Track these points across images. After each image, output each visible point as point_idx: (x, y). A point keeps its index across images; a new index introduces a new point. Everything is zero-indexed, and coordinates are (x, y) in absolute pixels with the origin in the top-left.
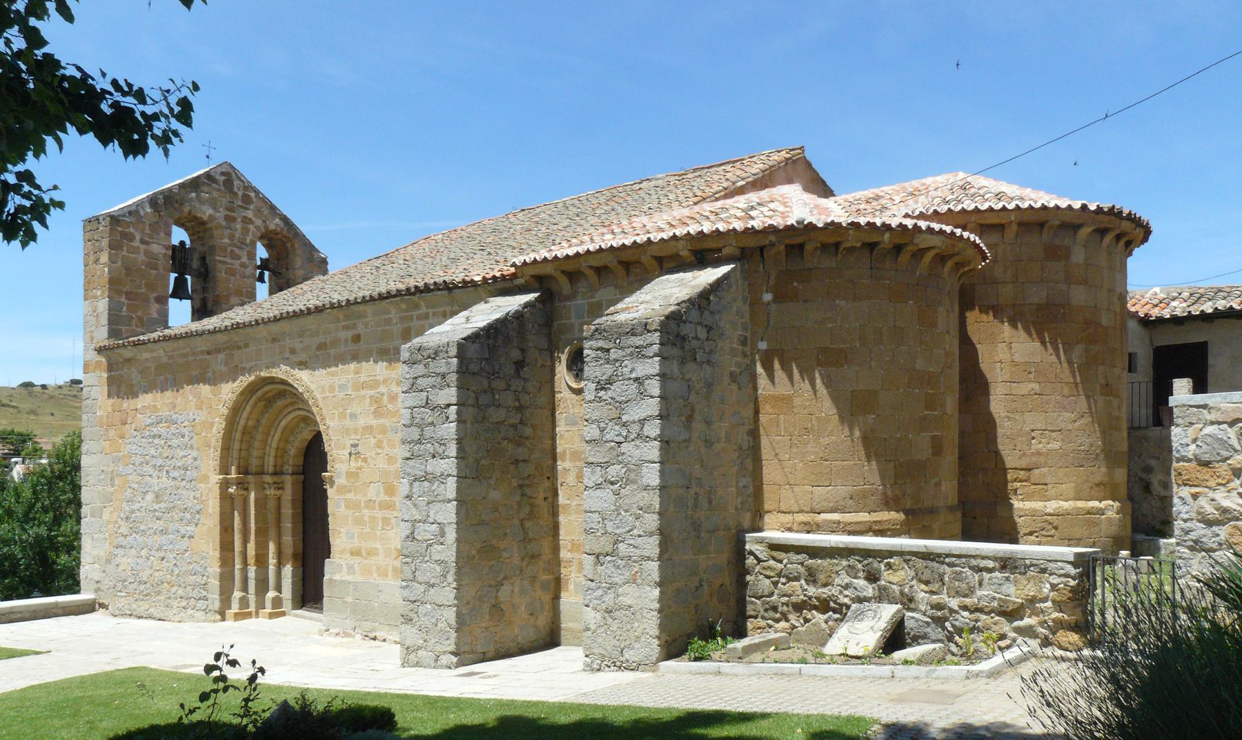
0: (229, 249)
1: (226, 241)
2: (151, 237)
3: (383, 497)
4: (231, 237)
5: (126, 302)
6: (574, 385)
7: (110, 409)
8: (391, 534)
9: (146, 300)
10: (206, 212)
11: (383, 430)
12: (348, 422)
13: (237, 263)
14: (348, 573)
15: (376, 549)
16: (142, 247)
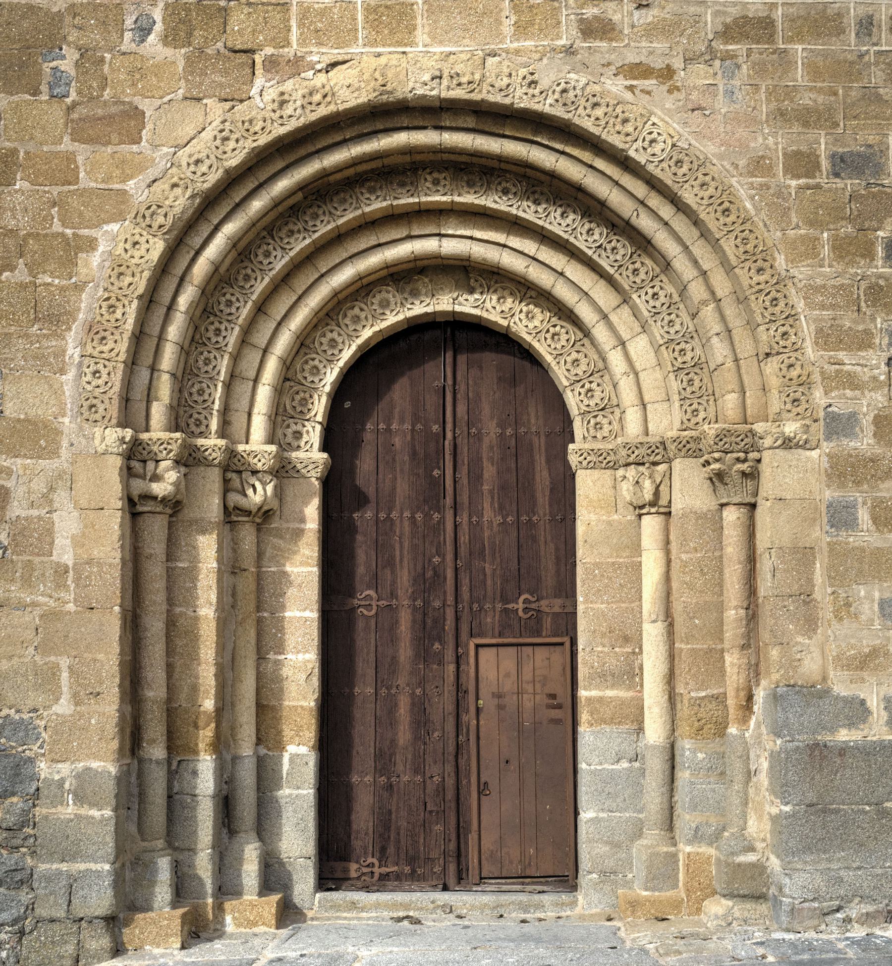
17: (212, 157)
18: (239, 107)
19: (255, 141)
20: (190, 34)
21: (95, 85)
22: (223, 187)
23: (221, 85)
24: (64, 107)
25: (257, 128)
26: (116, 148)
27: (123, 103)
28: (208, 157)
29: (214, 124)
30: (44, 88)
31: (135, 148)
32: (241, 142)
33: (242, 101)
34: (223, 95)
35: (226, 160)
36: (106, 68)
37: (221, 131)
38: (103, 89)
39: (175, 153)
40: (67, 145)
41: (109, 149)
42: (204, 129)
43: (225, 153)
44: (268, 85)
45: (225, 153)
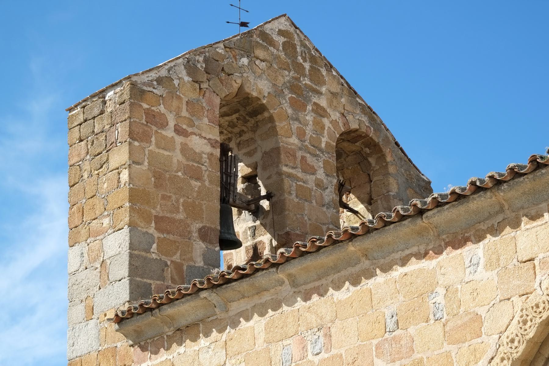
0: (299, 154)
1: (294, 140)
2: (192, 125)
4: (301, 135)
5: (156, 235)
10: (260, 87)
13: (311, 179)
16: (179, 140)
17: (519, 335)
18: (531, 297)
19: (541, 318)
20: (498, 260)
21: (455, 306)
22: (536, 350)
23: (519, 286)
24: (442, 325)
25: (541, 309)
26: (470, 343)
27: (470, 313)
28: (517, 335)
29: (518, 313)
30: (431, 316)
31: (479, 340)
32: (533, 321)
33: (531, 293)
34: (521, 293)
35: (527, 334)
36: (459, 294)
37: (522, 317)
38: (460, 308)
39: (500, 337)
40: (447, 347)
41: (467, 344)
42: (513, 317)
43: (526, 330)
44: (543, 278)
45: (526, 330)
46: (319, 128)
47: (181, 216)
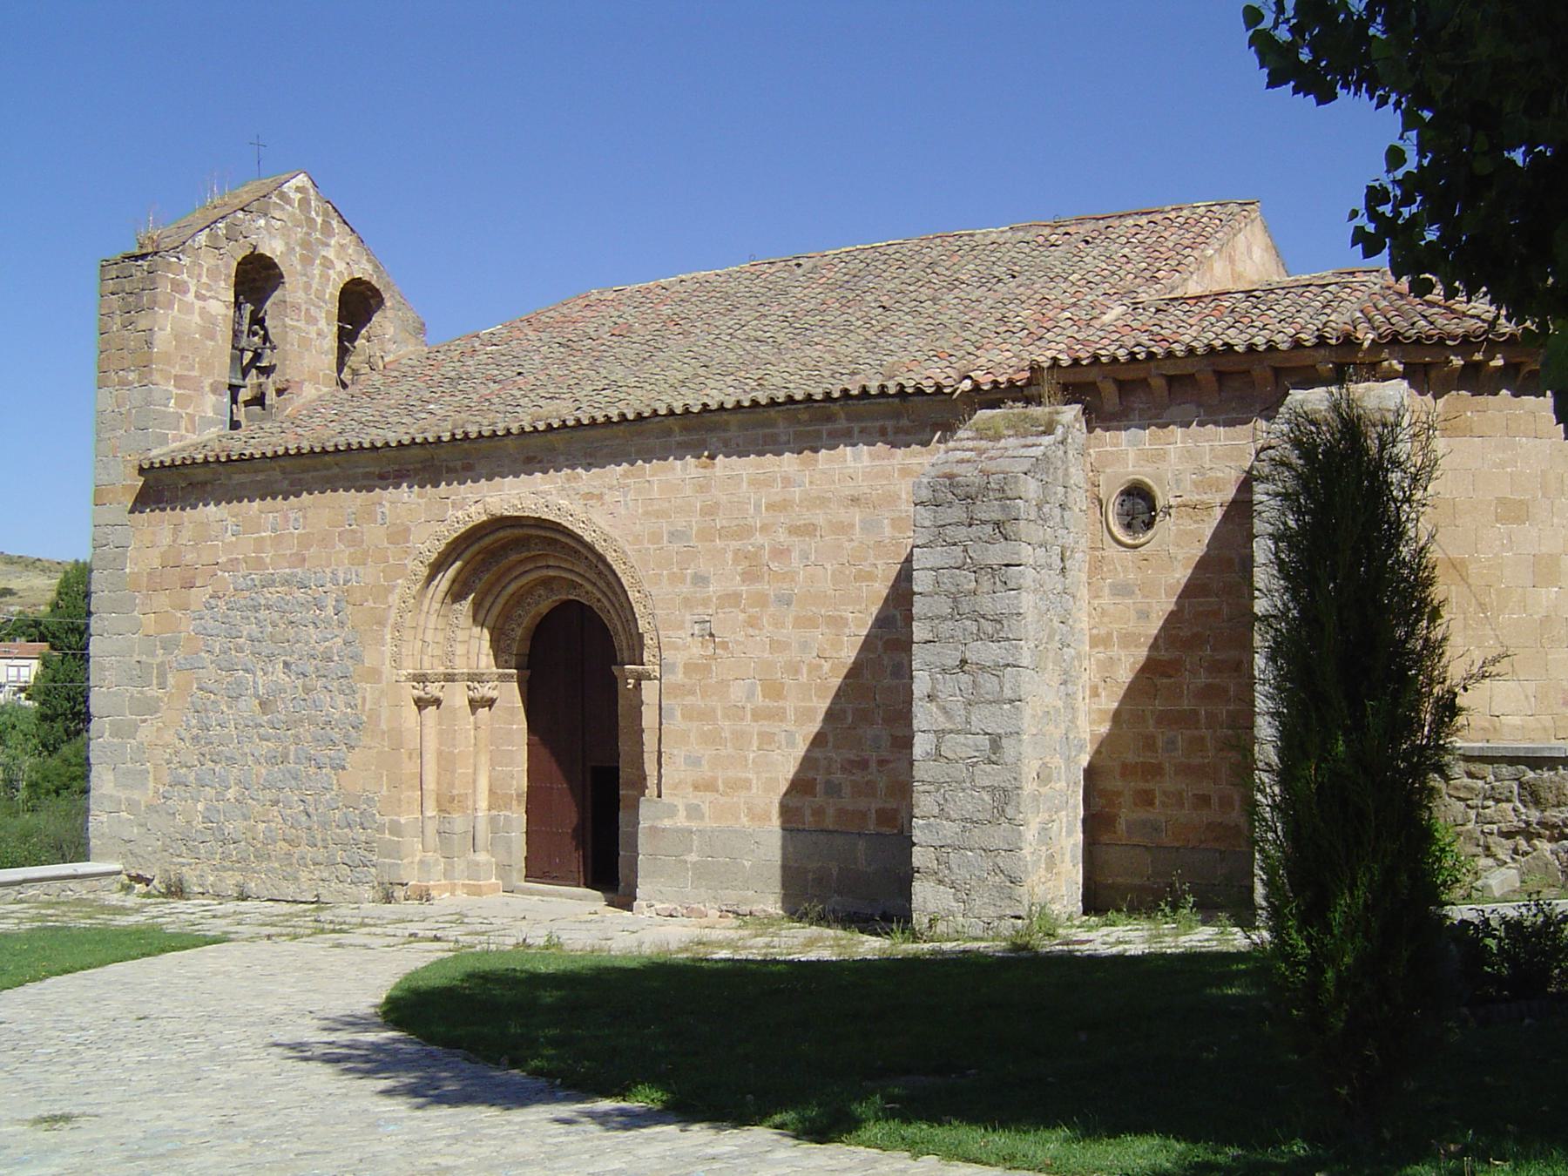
0: (303, 308)
1: (301, 294)
2: (209, 288)
3: (759, 700)
5: (175, 391)
6: (1129, 541)
7: (156, 563)
8: (776, 755)
9: (199, 388)
10: (273, 248)
11: (761, 600)
12: (686, 589)
13: (313, 330)
14: (689, 817)
15: (748, 781)
16: (198, 304)
46: (325, 277)
47: (196, 373)
